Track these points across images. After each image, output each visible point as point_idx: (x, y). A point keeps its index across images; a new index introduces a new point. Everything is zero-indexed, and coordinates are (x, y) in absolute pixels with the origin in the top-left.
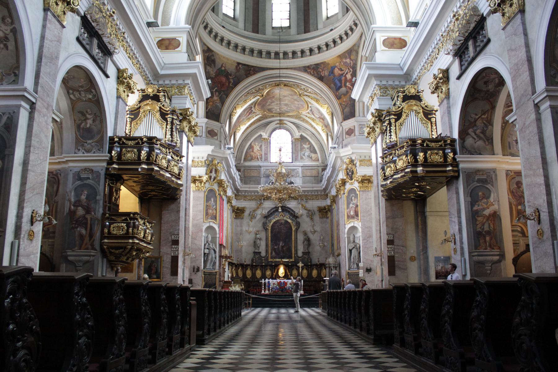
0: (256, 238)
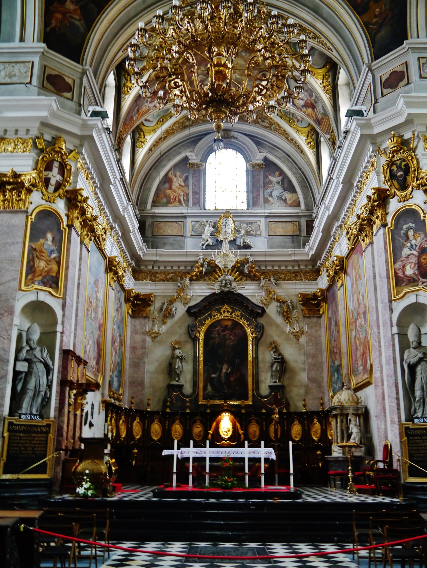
0: (173, 357)
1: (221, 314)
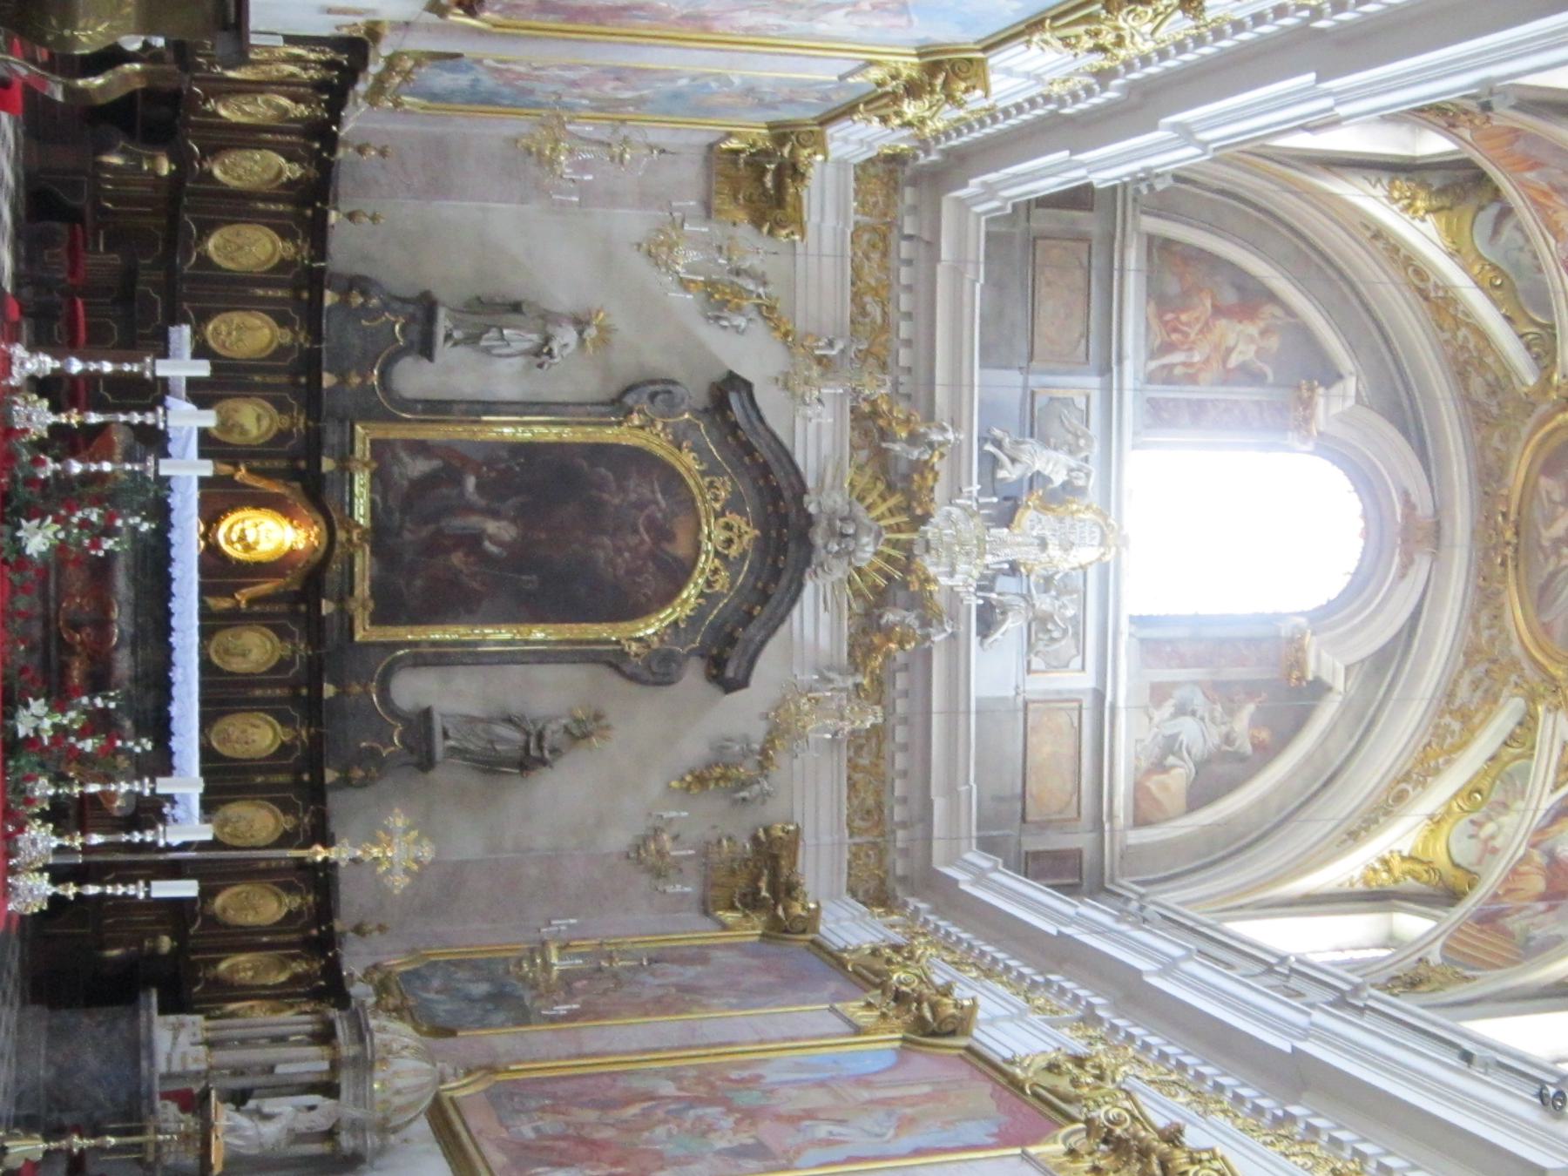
0: (547, 318)
1: (719, 515)
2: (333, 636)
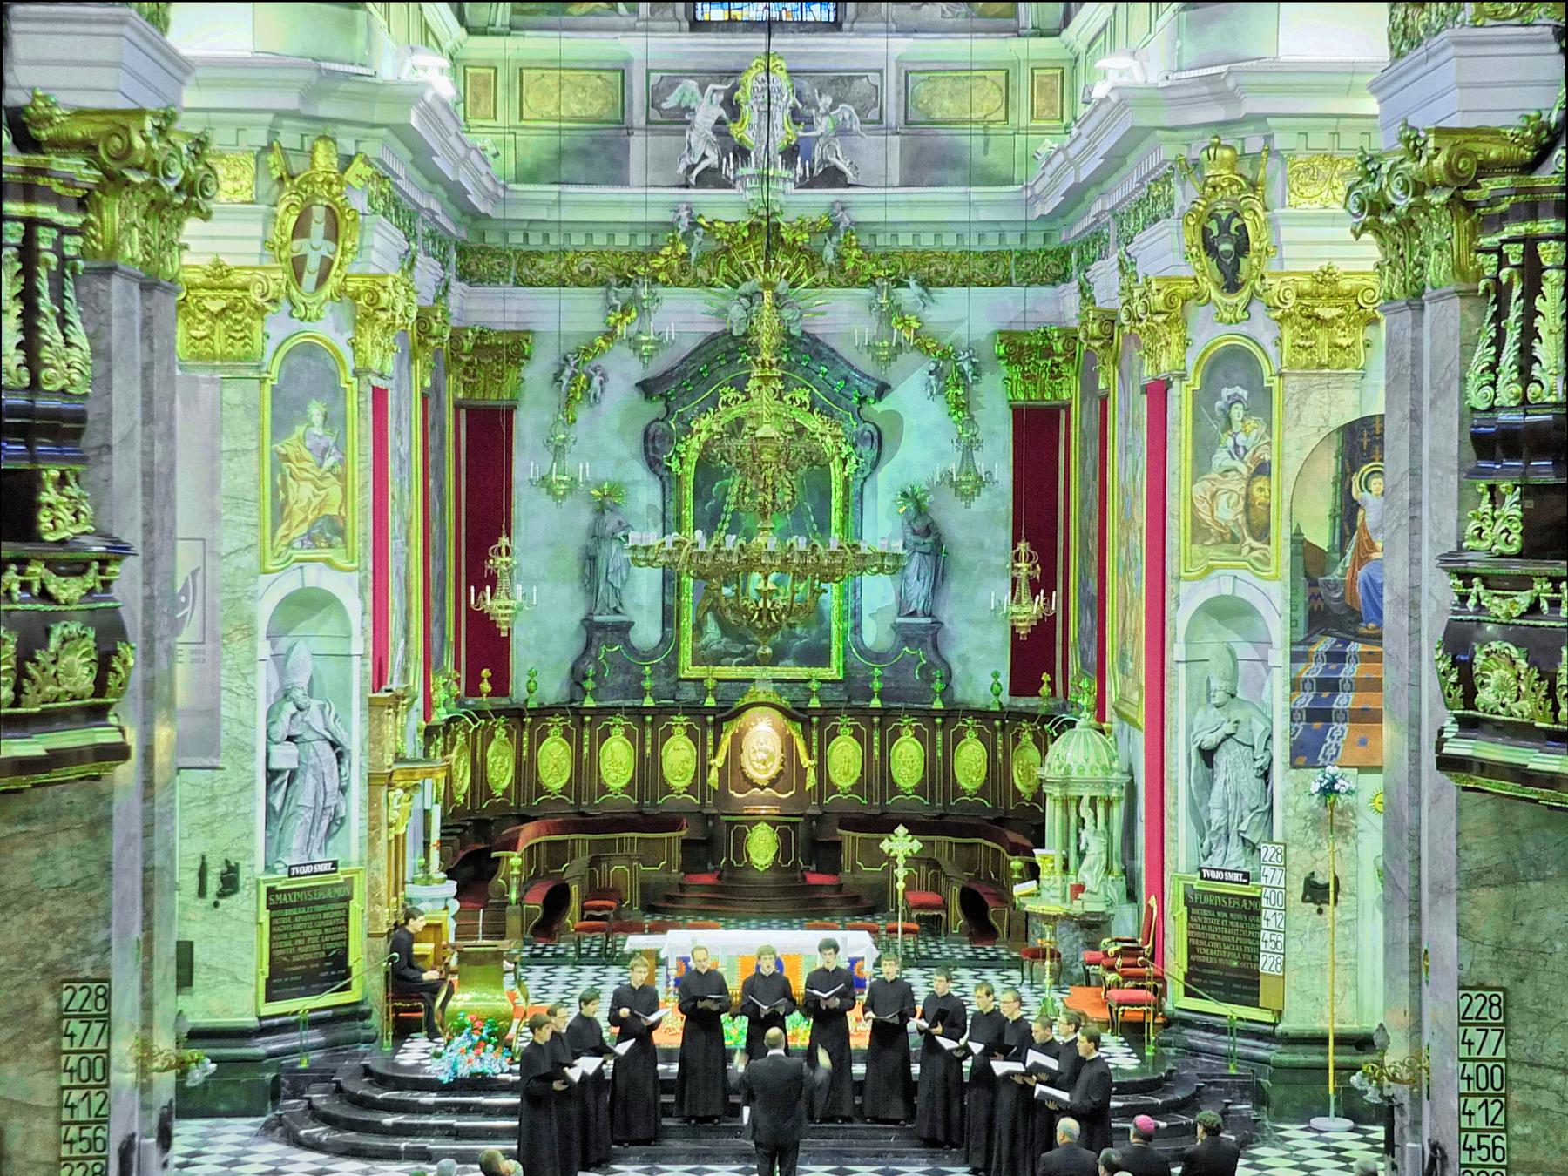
2: (836, 694)
